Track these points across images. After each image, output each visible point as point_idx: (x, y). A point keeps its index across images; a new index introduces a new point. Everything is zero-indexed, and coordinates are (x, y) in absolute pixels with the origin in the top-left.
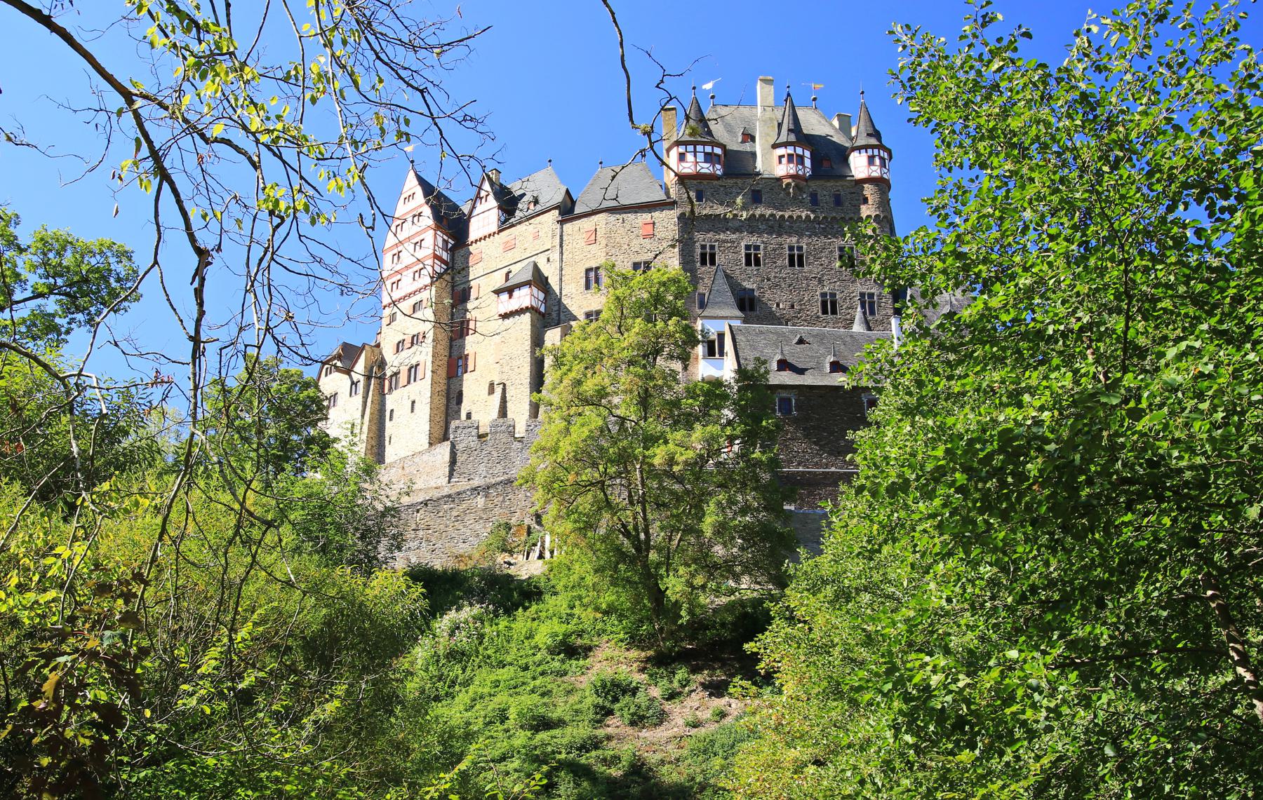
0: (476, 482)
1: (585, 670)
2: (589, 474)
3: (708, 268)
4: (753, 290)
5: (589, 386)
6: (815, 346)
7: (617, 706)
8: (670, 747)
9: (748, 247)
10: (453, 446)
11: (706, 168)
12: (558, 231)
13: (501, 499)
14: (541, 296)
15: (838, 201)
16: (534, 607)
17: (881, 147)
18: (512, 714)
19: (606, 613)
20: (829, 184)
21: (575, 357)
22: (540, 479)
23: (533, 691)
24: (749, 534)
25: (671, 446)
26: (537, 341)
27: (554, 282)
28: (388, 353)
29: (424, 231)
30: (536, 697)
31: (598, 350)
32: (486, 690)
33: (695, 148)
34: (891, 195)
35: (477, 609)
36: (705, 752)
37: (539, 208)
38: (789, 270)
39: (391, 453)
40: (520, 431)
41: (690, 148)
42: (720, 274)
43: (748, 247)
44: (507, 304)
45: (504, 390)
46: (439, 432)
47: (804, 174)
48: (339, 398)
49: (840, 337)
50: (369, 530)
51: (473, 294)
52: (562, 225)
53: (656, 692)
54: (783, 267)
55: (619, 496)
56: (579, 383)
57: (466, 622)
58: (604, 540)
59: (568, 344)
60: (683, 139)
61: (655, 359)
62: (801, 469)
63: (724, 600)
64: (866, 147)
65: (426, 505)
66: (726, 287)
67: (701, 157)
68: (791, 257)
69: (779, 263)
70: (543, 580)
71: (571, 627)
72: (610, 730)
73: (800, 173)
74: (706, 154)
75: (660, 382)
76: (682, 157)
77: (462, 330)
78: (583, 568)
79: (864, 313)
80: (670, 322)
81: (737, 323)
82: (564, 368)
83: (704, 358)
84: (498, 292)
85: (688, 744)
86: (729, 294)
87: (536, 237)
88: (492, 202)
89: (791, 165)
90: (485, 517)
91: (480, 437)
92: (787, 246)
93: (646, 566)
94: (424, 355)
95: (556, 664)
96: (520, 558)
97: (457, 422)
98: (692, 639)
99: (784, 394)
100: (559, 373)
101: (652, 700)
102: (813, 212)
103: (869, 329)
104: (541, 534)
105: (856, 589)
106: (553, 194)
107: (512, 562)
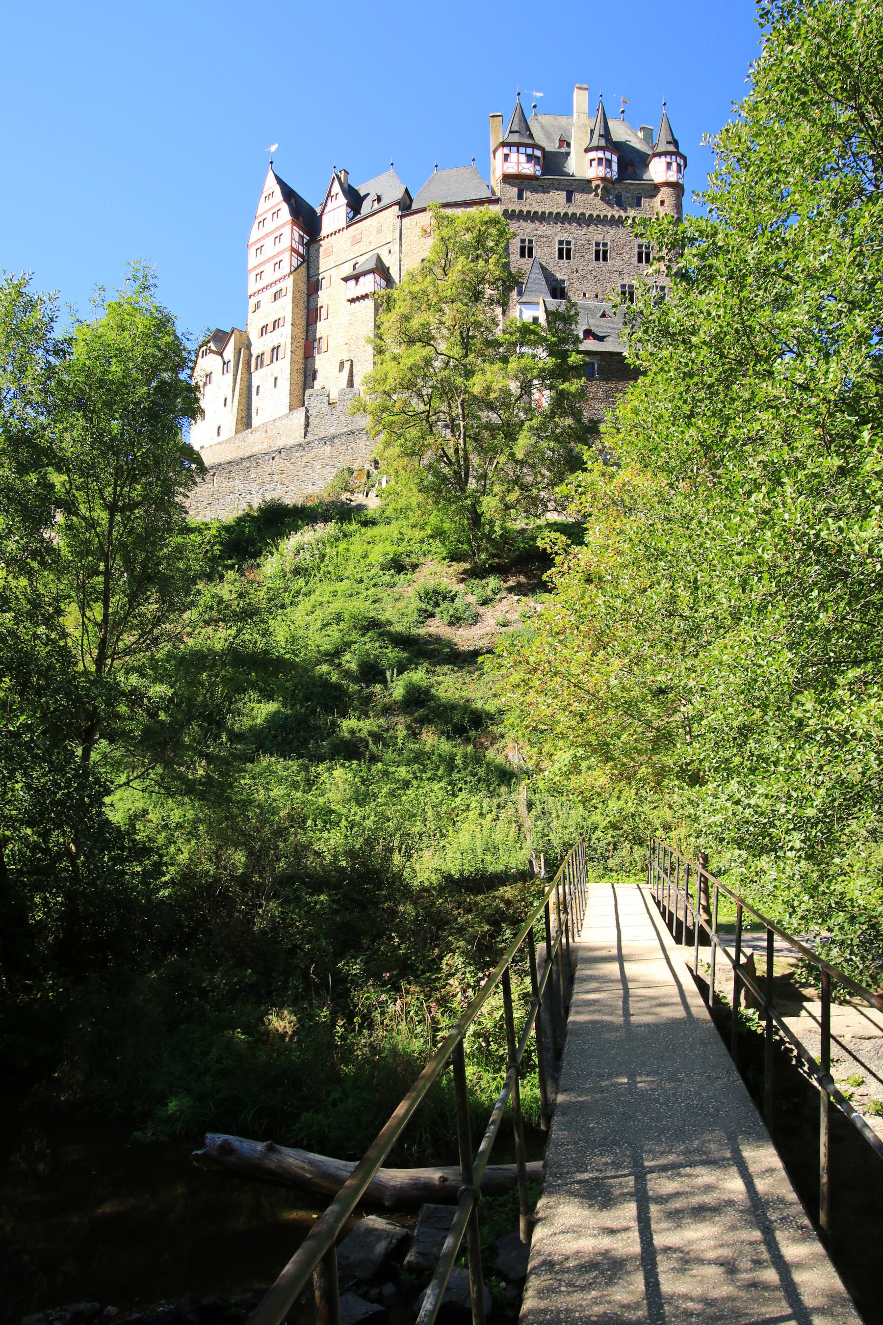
1: (410, 583)
7: (437, 610)
9: (561, 243)
10: (307, 411)
11: (528, 169)
29: (283, 226)
32: (325, 599)
37: (382, 204)
41: (514, 149)
42: (537, 265)
43: (561, 243)
45: (351, 366)
51: (324, 284)
56: (406, 318)
58: (430, 467)
64: (665, 154)
67: (523, 158)
69: (587, 257)
71: (401, 549)
73: (608, 176)
76: (506, 157)
84: (346, 279)
88: (342, 200)
94: (284, 336)
95: (387, 578)
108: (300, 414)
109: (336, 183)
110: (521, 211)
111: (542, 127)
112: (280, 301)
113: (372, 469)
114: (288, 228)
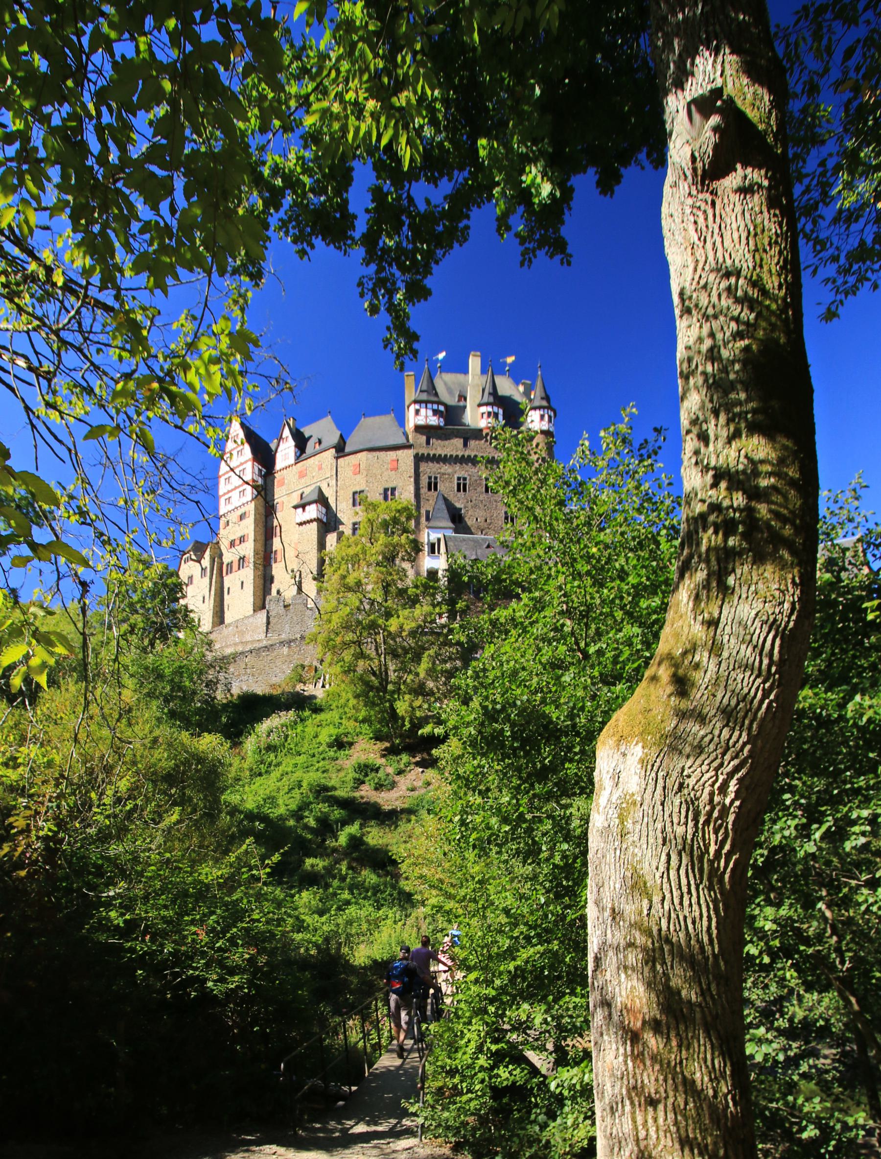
0: (284, 636)
1: (348, 757)
2: (350, 636)
3: (433, 493)
5: (351, 580)
9: (459, 479)
11: (434, 421)
14: (324, 510)
17: (549, 408)
18: (305, 784)
23: (317, 770)
26: (322, 545)
28: (224, 545)
29: (246, 462)
30: (319, 774)
32: (289, 769)
38: (484, 495)
41: (423, 405)
42: (441, 497)
46: (259, 603)
51: (279, 507)
55: (370, 650)
64: (539, 408)
66: (444, 507)
67: (430, 413)
71: (341, 731)
76: (417, 412)
78: (348, 695)
81: (450, 533)
84: (295, 507)
87: (320, 468)
88: (291, 443)
91: (285, 606)
94: (248, 549)
95: (331, 754)
96: (311, 687)
101: (388, 775)
106: (333, 437)
108: (262, 615)
109: (287, 428)
110: (429, 455)
111: (446, 384)
112: (244, 522)
113: (318, 665)
114: (250, 464)
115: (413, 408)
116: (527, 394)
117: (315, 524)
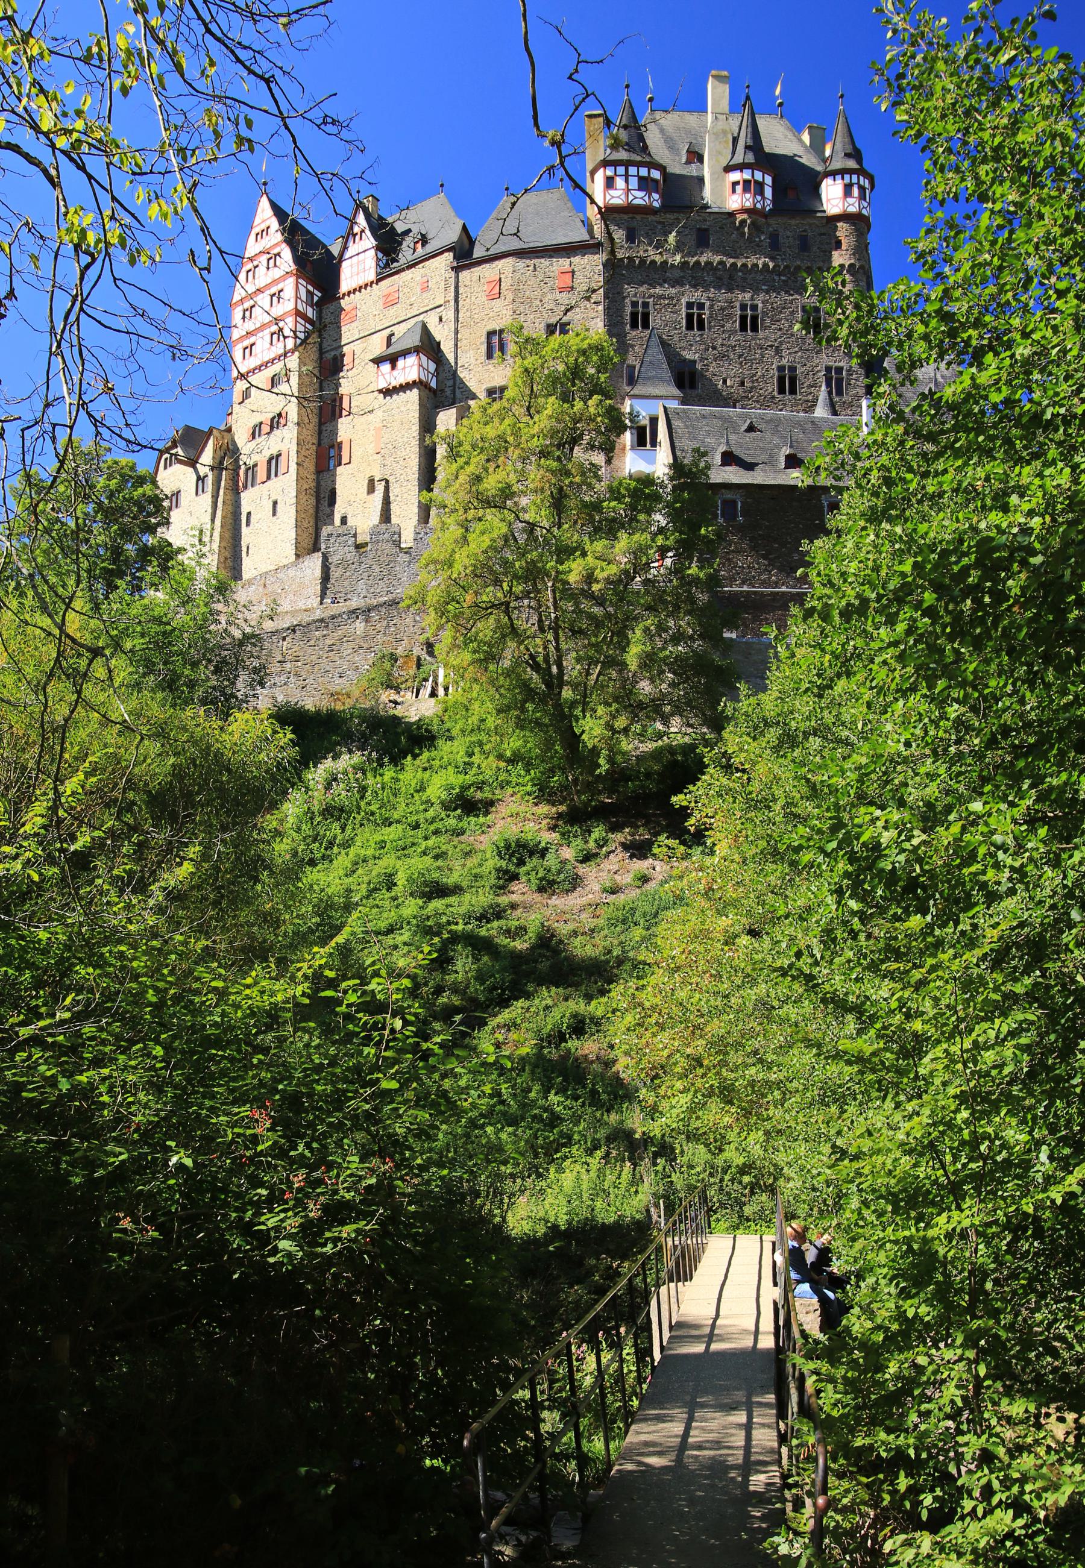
0: (355, 603)
2: (490, 594)
3: (639, 332)
4: (695, 362)
5: (491, 484)
6: (768, 435)
7: (523, 870)
8: (584, 916)
9: (690, 305)
10: (325, 558)
11: (639, 198)
12: (452, 281)
13: (385, 624)
14: (432, 367)
15: (804, 245)
16: (426, 755)
17: (861, 172)
18: (401, 879)
19: (511, 761)
20: (793, 222)
21: (474, 447)
22: (432, 598)
23: (424, 853)
24: (680, 666)
25: (590, 559)
26: (427, 426)
27: (447, 348)
28: (241, 437)
29: (282, 279)
30: (428, 861)
31: (502, 438)
32: (370, 852)
33: (627, 171)
34: (871, 238)
35: (357, 758)
36: (624, 921)
37: (430, 248)
39: (249, 567)
40: (407, 539)
41: (621, 170)
42: (655, 340)
43: (690, 305)
44: (387, 376)
46: (307, 542)
47: (764, 208)
48: (183, 494)
49: (799, 423)
50: (224, 661)
51: (346, 360)
52: (457, 273)
53: (568, 853)
54: (733, 332)
55: (527, 621)
56: (478, 479)
57: (345, 773)
58: (508, 673)
59: (465, 430)
60: (611, 158)
61: (572, 450)
62: (745, 588)
63: (649, 746)
64: (842, 172)
65: (294, 631)
66: (662, 358)
67: (634, 182)
68: (743, 319)
69: (728, 326)
70: (436, 721)
71: (469, 778)
72: (514, 898)
73: (759, 206)
74: (641, 179)
75: (578, 479)
76: (610, 183)
77: (334, 411)
79: (830, 393)
80: (590, 403)
81: (673, 405)
82: (461, 461)
83: (632, 448)
84: (377, 361)
85: (605, 913)
86: (665, 366)
87: (425, 289)
88: (369, 241)
89: (748, 196)
90: (365, 646)
91: (358, 547)
92: (738, 304)
93: (558, 706)
95: (452, 822)
96: (409, 696)
97: (330, 528)
98: (611, 792)
99: (729, 495)
100: (455, 466)
101: (564, 862)
102: (772, 259)
103: (835, 413)
104: (433, 667)
105: (804, 732)
107: (399, 700)
113: (424, 656)
114: (291, 281)
115: (600, 176)
116: (817, 147)
117: (415, 391)
